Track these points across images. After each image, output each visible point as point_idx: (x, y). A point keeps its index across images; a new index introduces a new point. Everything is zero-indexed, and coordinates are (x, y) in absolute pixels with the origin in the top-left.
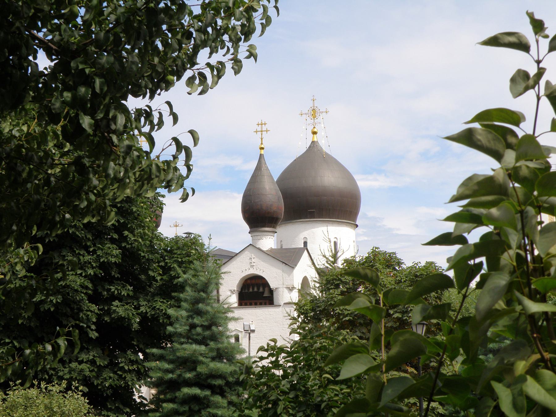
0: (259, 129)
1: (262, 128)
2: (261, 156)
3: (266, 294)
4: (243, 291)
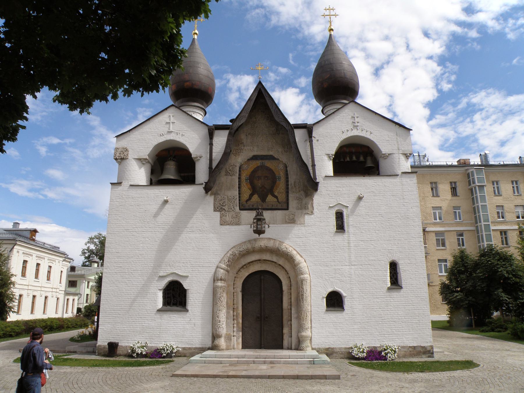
0: (327, 13)
1: (330, 12)
2: (331, 35)
3: (369, 164)
4: (337, 161)
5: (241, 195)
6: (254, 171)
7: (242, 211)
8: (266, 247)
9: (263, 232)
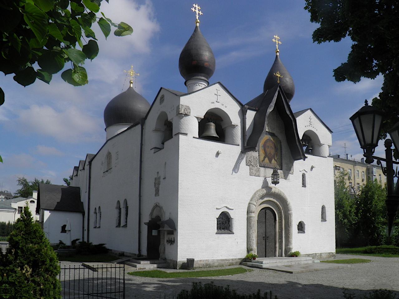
5: (260, 157)
6: (265, 142)
7: (261, 168)
8: (275, 192)
9: (278, 183)
